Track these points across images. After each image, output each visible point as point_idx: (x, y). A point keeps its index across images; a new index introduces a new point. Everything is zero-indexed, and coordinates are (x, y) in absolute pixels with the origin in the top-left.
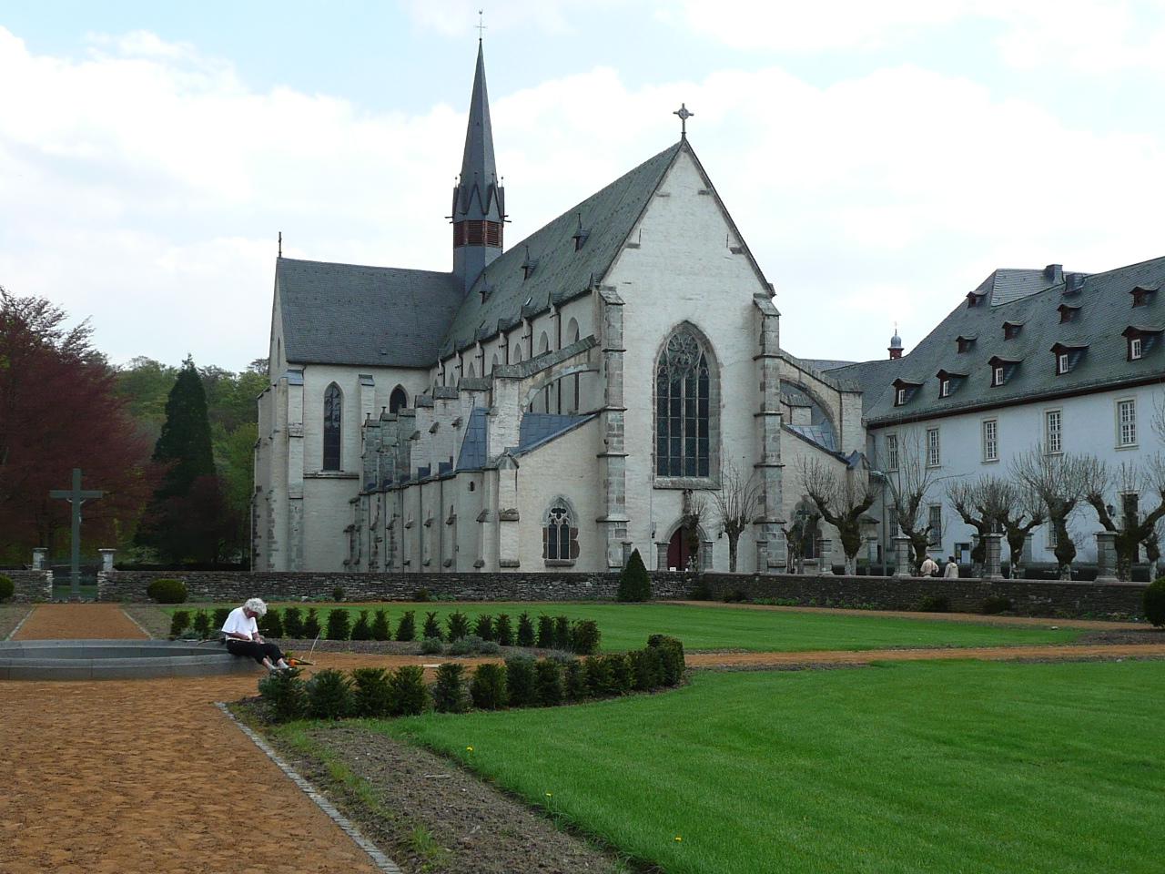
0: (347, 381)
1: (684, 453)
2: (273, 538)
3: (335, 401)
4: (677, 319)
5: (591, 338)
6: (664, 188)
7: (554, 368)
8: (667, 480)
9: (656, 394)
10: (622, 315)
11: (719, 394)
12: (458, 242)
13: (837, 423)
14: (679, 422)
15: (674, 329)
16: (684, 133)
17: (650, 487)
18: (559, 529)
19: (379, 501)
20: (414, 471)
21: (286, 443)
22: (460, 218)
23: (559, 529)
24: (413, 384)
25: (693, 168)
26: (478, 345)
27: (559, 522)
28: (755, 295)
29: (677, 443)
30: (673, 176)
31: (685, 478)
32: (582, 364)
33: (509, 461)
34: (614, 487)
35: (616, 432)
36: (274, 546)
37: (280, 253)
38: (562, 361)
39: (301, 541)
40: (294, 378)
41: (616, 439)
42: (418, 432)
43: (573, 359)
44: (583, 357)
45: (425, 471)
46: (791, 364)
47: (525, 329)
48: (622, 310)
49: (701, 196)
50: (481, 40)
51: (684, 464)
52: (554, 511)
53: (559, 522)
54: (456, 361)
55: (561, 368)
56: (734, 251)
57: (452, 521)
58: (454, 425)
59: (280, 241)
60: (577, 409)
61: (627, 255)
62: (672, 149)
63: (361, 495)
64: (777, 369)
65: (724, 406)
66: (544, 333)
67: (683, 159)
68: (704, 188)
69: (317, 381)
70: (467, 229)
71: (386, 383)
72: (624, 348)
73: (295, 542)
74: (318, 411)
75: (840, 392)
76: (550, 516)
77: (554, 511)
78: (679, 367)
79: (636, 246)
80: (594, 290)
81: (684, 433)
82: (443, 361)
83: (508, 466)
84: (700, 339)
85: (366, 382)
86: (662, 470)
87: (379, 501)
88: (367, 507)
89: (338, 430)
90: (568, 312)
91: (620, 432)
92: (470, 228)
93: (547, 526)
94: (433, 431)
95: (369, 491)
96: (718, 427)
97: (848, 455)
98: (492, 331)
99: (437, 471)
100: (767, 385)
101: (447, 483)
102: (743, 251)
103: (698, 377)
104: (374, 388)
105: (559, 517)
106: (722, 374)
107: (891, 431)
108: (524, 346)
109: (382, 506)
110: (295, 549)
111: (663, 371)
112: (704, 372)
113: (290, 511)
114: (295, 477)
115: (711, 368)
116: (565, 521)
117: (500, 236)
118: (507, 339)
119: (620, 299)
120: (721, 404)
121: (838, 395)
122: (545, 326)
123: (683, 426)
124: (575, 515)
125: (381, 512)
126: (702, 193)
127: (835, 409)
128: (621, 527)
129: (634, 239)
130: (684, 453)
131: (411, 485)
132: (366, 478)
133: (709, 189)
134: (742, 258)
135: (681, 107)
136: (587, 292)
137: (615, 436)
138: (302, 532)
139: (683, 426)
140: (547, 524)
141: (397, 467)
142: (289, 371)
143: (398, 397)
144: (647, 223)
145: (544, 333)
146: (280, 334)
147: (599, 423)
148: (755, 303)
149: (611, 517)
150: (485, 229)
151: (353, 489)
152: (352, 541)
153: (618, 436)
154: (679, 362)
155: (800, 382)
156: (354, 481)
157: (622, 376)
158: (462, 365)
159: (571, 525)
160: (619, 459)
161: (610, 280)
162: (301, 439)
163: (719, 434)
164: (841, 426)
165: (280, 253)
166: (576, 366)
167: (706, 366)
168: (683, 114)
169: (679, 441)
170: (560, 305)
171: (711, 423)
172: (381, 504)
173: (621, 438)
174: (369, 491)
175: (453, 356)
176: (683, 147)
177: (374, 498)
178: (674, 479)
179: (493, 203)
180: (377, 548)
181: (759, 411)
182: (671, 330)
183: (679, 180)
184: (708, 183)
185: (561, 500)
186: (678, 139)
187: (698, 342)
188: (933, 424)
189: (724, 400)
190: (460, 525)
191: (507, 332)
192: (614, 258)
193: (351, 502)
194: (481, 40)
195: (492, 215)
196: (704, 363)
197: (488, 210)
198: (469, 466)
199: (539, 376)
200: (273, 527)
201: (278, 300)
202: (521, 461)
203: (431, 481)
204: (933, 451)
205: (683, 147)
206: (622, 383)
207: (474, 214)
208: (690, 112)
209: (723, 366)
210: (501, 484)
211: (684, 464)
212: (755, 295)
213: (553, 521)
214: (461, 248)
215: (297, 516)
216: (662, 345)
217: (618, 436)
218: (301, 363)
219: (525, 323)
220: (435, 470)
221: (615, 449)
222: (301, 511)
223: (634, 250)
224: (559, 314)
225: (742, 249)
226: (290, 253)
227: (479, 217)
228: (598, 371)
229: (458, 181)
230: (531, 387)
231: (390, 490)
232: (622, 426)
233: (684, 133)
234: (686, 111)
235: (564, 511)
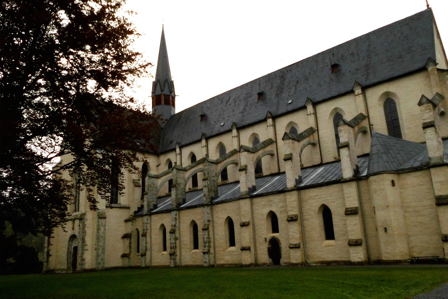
2: (85, 242)
16: (428, 6)
19: (176, 215)
22: (158, 92)
36: (86, 248)
39: (104, 244)
42: (246, 166)
50: (163, 25)
70: (163, 98)
73: (101, 244)
88: (149, 222)
92: (165, 97)
109: (178, 219)
110: (101, 248)
113: (98, 226)
125: (178, 222)
138: (105, 239)
150: (171, 99)
151: (126, 214)
152: (130, 243)
156: (127, 210)
172: (177, 217)
180: (176, 243)
193: (126, 221)
194: (163, 25)
195: (173, 94)
200: (85, 235)
214: (159, 107)
215: (102, 229)
222: (105, 225)
227: (169, 93)
233: (428, 6)
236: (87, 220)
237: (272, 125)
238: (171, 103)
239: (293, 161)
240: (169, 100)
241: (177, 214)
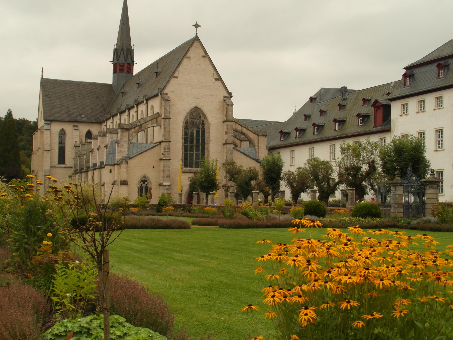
0: (68, 128)
1: (194, 159)
3: (63, 136)
4: (193, 106)
5: (158, 113)
6: (188, 55)
7: (143, 125)
8: (187, 169)
9: (184, 135)
10: (170, 105)
11: (209, 136)
12: (115, 71)
13: (256, 147)
14: (193, 146)
15: (191, 110)
16: (197, 33)
17: (181, 171)
18: (144, 188)
20: (91, 165)
21: (43, 153)
22: (116, 62)
23: (144, 188)
24: (95, 130)
25: (200, 47)
26: (119, 114)
27: (144, 185)
28: (225, 97)
29: (192, 155)
30: (193, 49)
31: (195, 169)
32: (154, 124)
33: (124, 161)
34: (166, 172)
35: (166, 150)
37: (42, 76)
38: (146, 122)
40: (47, 127)
41: (166, 153)
42: (93, 149)
43: (150, 122)
44: (155, 120)
45: (95, 165)
46: (238, 124)
47: (135, 109)
48: (169, 102)
49: (203, 58)
51: (194, 163)
52: (142, 181)
53: (144, 185)
54: (111, 121)
55: (146, 125)
56: (216, 79)
57: (103, 185)
58: (105, 147)
59: (42, 71)
60: (153, 141)
61: (173, 81)
62: (192, 39)
63: (73, 174)
64: (232, 126)
65: (211, 140)
66: (142, 111)
67: (196, 44)
68: (204, 54)
69: (56, 128)
70: (118, 66)
71: (84, 129)
72: (171, 117)
74: (56, 140)
75: (258, 135)
76: (141, 183)
77: (142, 181)
78: (194, 124)
79: (177, 77)
80: (159, 95)
81: (195, 151)
82: (107, 120)
83: (124, 163)
84: (202, 114)
85: (76, 128)
86: (186, 164)
87: (79, 176)
89: (64, 148)
90: (151, 103)
91: (168, 150)
93: (139, 187)
94: (98, 149)
95: (76, 172)
96: (208, 148)
97: (261, 160)
98: (124, 109)
99: (99, 165)
100: (228, 132)
101: (103, 170)
102: (220, 79)
103: (200, 129)
104: (78, 131)
105: (144, 183)
106: (210, 128)
107: (278, 151)
108: (135, 115)
111: (187, 126)
112: (203, 127)
114: (47, 166)
115: (206, 125)
116: (146, 185)
117: (132, 69)
118: (129, 112)
119: (169, 98)
120: (210, 139)
121: (257, 136)
122: (142, 107)
123: (194, 148)
124: (151, 183)
126: (204, 57)
127: (256, 142)
128: (168, 187)
129: (176, 75)
130: (194, 159)
131: (90, 170)
132: (75, 167)
133: (206, 55)
134: (219, 83)
135: (196, 23)
136: (157, 95)
137: (166, 152)
139: (194, 148)
140: (139, 186)
141: (85, 163)
142: (45, 124)
143: (89, 135)
144: (181, 68)
145: (142, 111)
146: (41, 109)
147: (160, 147)
148: (224, 100)
149: (164, 184)
150: (125, 66)
153: (167, 152)
154: (193, 123)
155: (242, 131)
156: (71, 169)
157: (169, 128)
158: (113, 122)
159: (149, 186)
160: (168, 161)
161: (166, 91)
162: (49, 152)
163: (209, 151)
164: (258, 149)
165: (42, 76)
166: (152, 124)
167: (204, 124)
168: (197, 26)
169: (193, 154)
170: (147, 100)
171: (206, 147)
172: (80, 178)
173: (169, 153)
174: (76, 172)
175: (109, 118)
176: (196, 39)
177: (78, 175)
178: (191, 169)
179: (129, 56)
181: (224, 142)
182: (190, 110)
183: (194, 52)
184: (206, 53)
185: (145, 177)
186: (194, 35)
187: (201, 115)
188: (292, 148)
189: (211, 138)
190: (106, 186)
191: (129, 109)
192: (168, 82)
195: (129, 61)
196: (203, 123)
197: (127, 59)
198: (110, 163)
199: (137, 128)
201: (41, 95)
202: (129, 162)
203: (97, 169)
204: (293, 158)
205: (196, 39)
206: (169, 131)
207: (122, 60)
208: (199, 25)
209: (210, 124)
210: (121, 170)
211: (194, 163)
212: (225, 97)
213: (142, 185)
216: (186, 116)
217: (167, 152)
218: (49, 120)
219: (135, 106)
220: (98, 165)
221: (166, 157)
223: (176, 79)
224: (147, 103)
225: (219, 79)
226: (47, 76)
227: (124, 61)
228: (161, 126)
229: (115, 47)
230: (134, 132)
231: (83, 172)
232: (169, 148)
233: (197, 33)
234: (198, 25)
235: (146, 181)
236: (39, 176)
237: (127, 115)
238: (126, 70)
239: (100, 151)
240: (124, 67)
241: (80, 176)
